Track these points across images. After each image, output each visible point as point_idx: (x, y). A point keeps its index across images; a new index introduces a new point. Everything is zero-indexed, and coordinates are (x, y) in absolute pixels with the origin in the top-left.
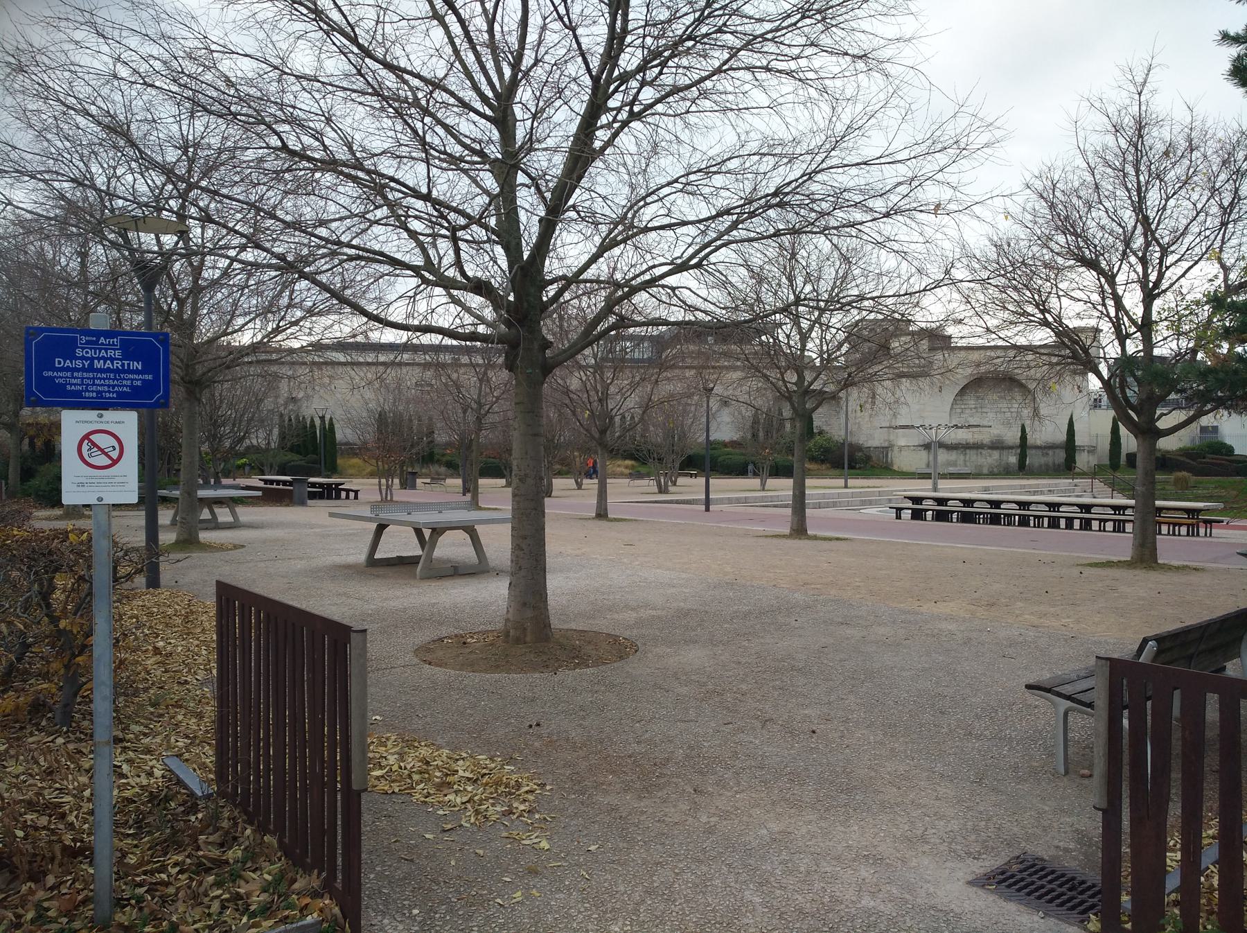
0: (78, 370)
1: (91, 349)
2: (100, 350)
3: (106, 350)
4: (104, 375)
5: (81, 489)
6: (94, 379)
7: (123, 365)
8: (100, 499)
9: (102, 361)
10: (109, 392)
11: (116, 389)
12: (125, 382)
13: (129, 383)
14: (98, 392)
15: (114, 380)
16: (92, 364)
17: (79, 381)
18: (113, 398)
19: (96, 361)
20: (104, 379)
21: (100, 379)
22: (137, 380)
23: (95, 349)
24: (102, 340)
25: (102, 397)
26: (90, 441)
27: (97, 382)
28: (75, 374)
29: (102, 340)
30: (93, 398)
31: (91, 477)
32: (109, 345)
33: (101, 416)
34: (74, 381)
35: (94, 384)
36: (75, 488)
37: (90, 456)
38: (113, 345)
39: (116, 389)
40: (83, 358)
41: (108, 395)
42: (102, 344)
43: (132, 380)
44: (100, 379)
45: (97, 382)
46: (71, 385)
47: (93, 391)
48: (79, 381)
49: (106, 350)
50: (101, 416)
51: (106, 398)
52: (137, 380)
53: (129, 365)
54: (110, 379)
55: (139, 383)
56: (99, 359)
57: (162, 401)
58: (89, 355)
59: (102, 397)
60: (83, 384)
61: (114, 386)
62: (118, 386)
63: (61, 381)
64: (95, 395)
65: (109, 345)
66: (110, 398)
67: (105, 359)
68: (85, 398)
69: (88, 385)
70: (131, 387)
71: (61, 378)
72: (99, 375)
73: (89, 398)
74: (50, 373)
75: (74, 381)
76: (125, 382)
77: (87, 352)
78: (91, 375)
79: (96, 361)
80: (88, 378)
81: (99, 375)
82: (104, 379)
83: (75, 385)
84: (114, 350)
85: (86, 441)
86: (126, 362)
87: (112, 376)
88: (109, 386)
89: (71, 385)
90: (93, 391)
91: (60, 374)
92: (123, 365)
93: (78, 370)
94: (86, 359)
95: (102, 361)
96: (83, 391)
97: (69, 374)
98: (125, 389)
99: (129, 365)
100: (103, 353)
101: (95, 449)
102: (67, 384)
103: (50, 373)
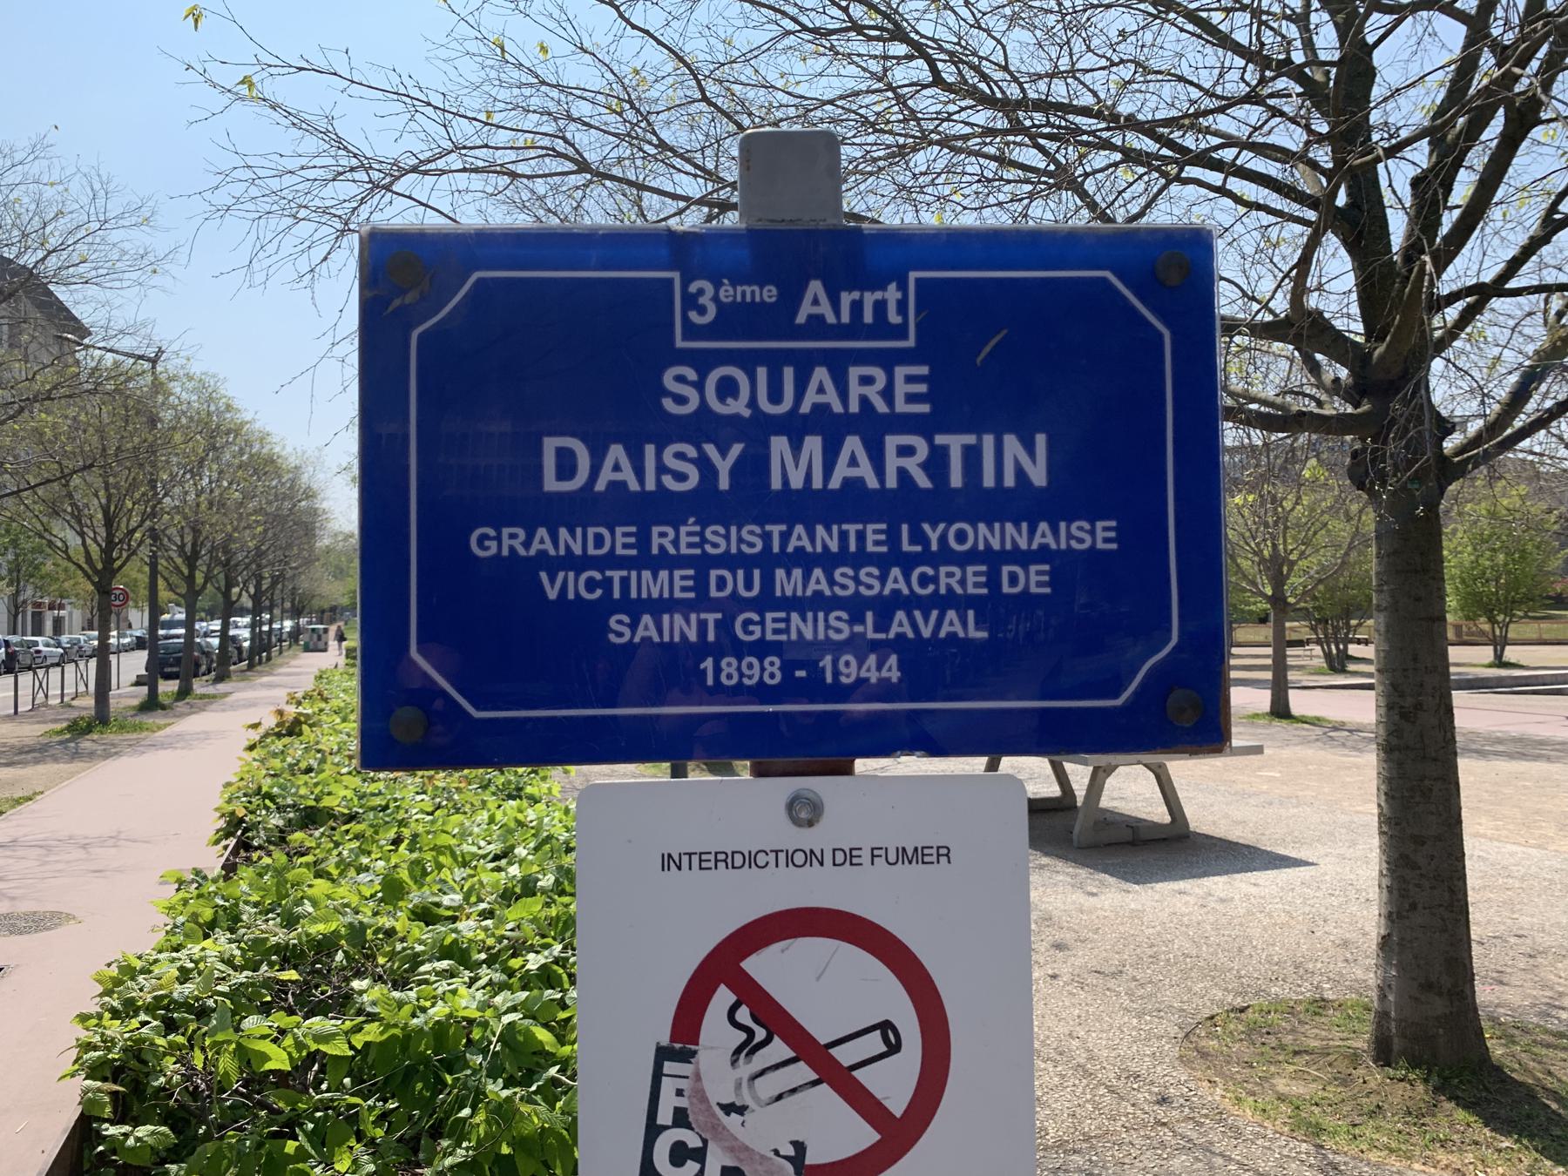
1: (747, 361)
2: (804, 364)
3: (838, 364)
4: (826, 538)
6: (767, 561)
7: (937, 463)
9: (813, 445)
11: (900, 624)
12: (949, 578)
13: (973, 580)
14: (797, 656)
16: (754, 467)
17: (679, 583)
19: (779, 445)
20: (829, 561)
21: (804, 560)
22: (1023, 558)
23: (775, 361)
24: (815, 301)
25: (816, 688)
26: (751, 994)
27: (788, 583)
28: (661, 538)
29: (815, 301)
30: (762, 692)
32: (855, 329)
33: (805, 812)
34: (652, 585)
35: (766, 601)
38: (881, 328)
39: (900, 624)
40: (703, 427)
41: (850, 671)
42: (817, 326)
43: (992, 559)
44: (804, 560)
45: (788, 583)
46: (636, 609)
47: (762, 649)
48: (679, 583)
49: (838, 364)
50: (805, 812)
52: (1023, 558)
53: (972, 456)
54: (860, 559)
55: (1035, 579)
56: (795, 426)
58: (738, 406)
59: (816, 688)
60: (702, 601)
61: (885, 608)
62: (909, 603)
63: (576, 585)
64: (773, 664)
65: (855, 329)
67: (832, 428)
68: (720, 692)
69: (736, 603)
70: (990, 607)
71: (578, 563)
73: (738, 692)
74: (512, 540)
75: (652, 585)
76: (949, 578)
77: (727, 388)
78: (750, 539)
79: (779, 445)
80: (730, 561)
82: (829, 561)
83: (659, 607)
84: (887, 361)
85: (723, 997)
86: (955, 443)
87: (874, 535)
88: (856, 608)
89: (636, 609)
90: (762, 649)
91: (571, 541)
92: (937, 463)
95: (813, 445)
96: (703, 649)
97: (621, 540)
98: (952, 623)
99: (972, 456)
100: (821, 390)
101: (779, 1049)
102: (608, 606)
103: (512, 540)
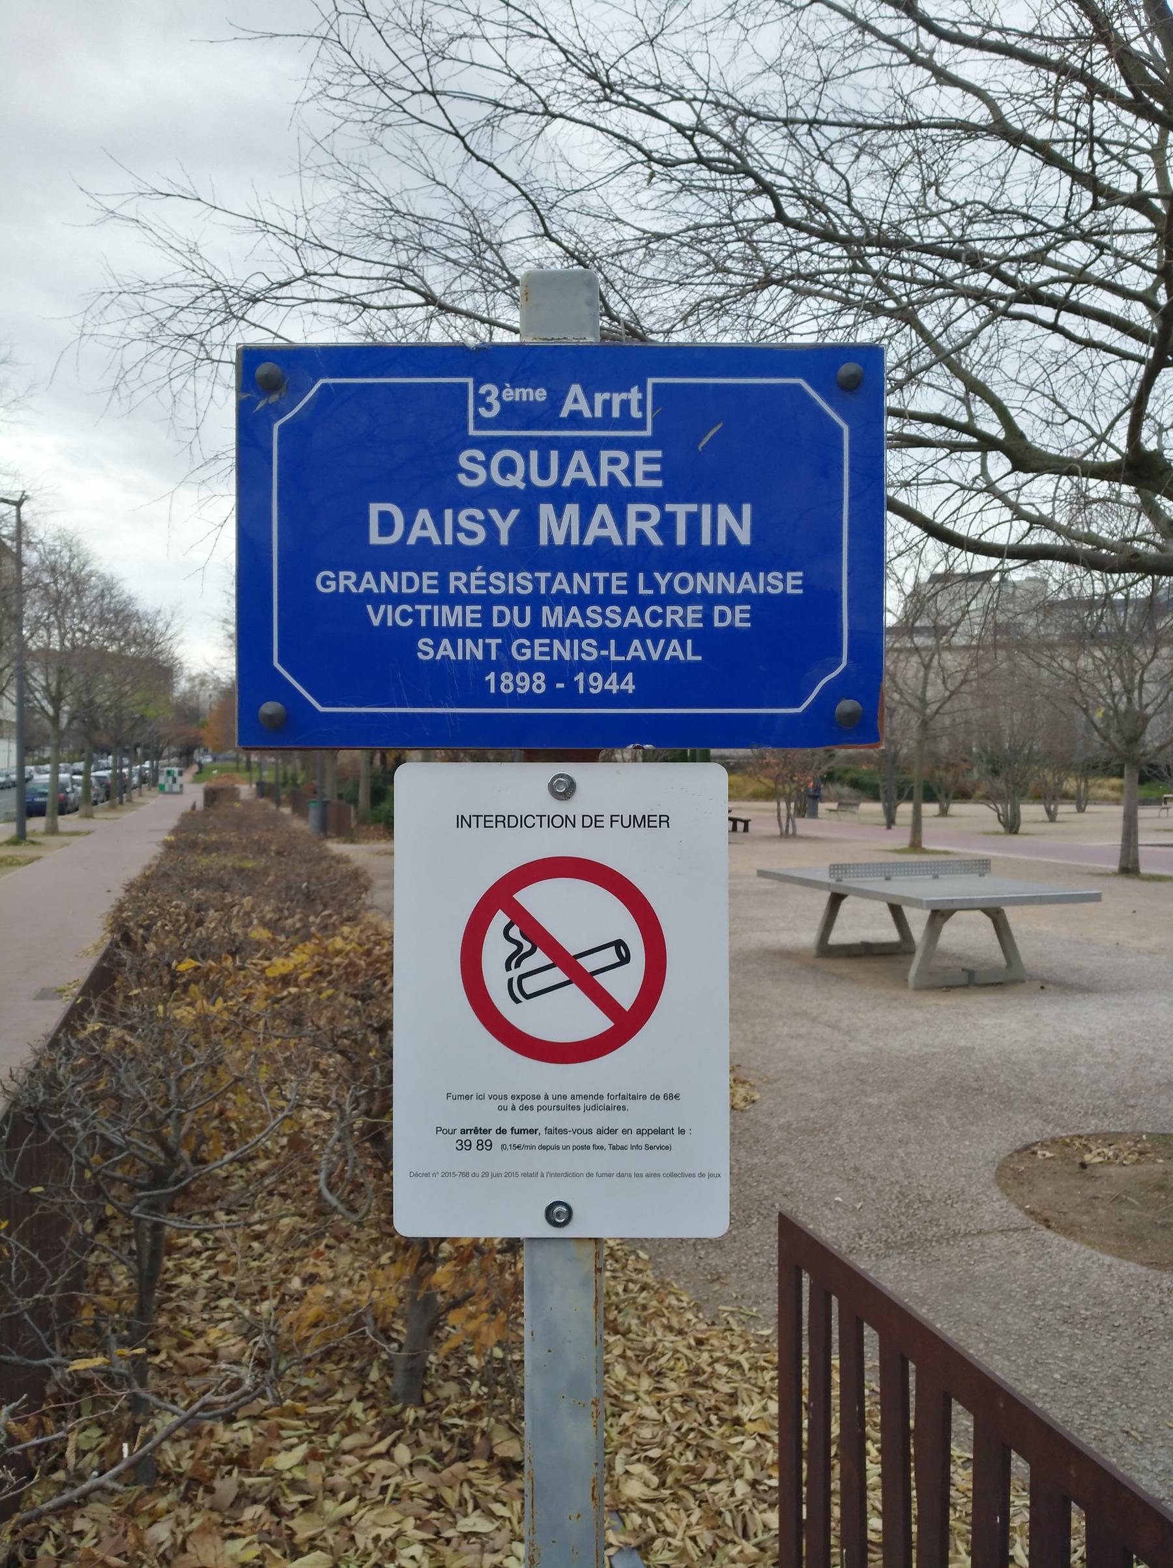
0: (464, 558)
1: (522, 445)
2: (566, 449)
3: (592, 449)
4: (582, 584)
5: (474, 1160)
6: (536, 601)
7: (667, 525)
8: (558, 1213)
9: (572, 511)
10: (604, 667)
11: (636, 650)
12: (673, 615)
13: (691, 617)
14: (557, 670)
15: (624, 603)
16: (528, 524)
17: (469, 616)
18: (621, 699)
19: (546, 511)
20: (582, 601)
21: (564, 600)
22: (731, 600)
23: (544, 446)
24: (575, 400)
25: (571, 697)
26: (520, 916)
27: (551, 617)
28: (457, 581)
29: (575, 400)
30: (530, 699)
31: (524, 1101)
32: (607, 422)
33: (564, 790)
34: (450, 617)
35: (536, 631)
36: (445, 1152)
37: (517, 991)
38: (627, 421)
39: (636, 650)
40: (489, 496)
41: (597, 684)
42: (576, 419)
43: (708, 600)
44: (564, 600)
45: (551, 617)
46: (437, 634)
47: (531, 667)
48: (469, 616)
49: (592, 449)
50: (564, 790)
51: (589, 700)
52: (731, 600)
53: (694, 521)
54: (606, 600)
55: (738, 617)
56: (559, 497)
57: (847, 706)
58: (515, 481)
59: (571, 697)
60: (487, 631)
61: (624, 637)
62: (642, 633)
63: (393, 616)
64: (540, 678)
65: (607, 422)
66: (606, 698)
67: (586, 497)
68: (500, 699)
69: (509, 634)
70: (704, 638)
71: (395, 599)
72: (561, 583)
73: (515, 699)
74: (346, 581)
75: (450, 617)
76: (673, 615)
77: (508, 467)
78: (523, 583)
79: (546, 511)
80: (509, 600)
81: (561, 583)
82: (582, 601)
83: (454, 634)
84: (630, 446)
85: (501, 919)
86: (681, 510)
87: (618, 580)
88: (602, 636)
89: (437, 634)
90: (531, 667)
91: (390, 582)
92: (667, 525)
93: (464, 558)
94: (502, 498)
95: (572, 511)
96: (487, 665)
97: (427, 582)
98: (675, 650)
99: (694, 521)
100: (579, 468)
101: (540, 958)
102: (416, 632)
103: (346, 581)
